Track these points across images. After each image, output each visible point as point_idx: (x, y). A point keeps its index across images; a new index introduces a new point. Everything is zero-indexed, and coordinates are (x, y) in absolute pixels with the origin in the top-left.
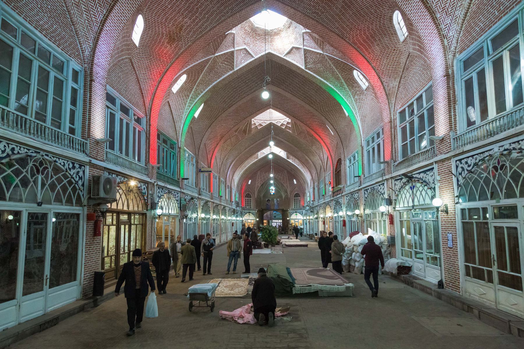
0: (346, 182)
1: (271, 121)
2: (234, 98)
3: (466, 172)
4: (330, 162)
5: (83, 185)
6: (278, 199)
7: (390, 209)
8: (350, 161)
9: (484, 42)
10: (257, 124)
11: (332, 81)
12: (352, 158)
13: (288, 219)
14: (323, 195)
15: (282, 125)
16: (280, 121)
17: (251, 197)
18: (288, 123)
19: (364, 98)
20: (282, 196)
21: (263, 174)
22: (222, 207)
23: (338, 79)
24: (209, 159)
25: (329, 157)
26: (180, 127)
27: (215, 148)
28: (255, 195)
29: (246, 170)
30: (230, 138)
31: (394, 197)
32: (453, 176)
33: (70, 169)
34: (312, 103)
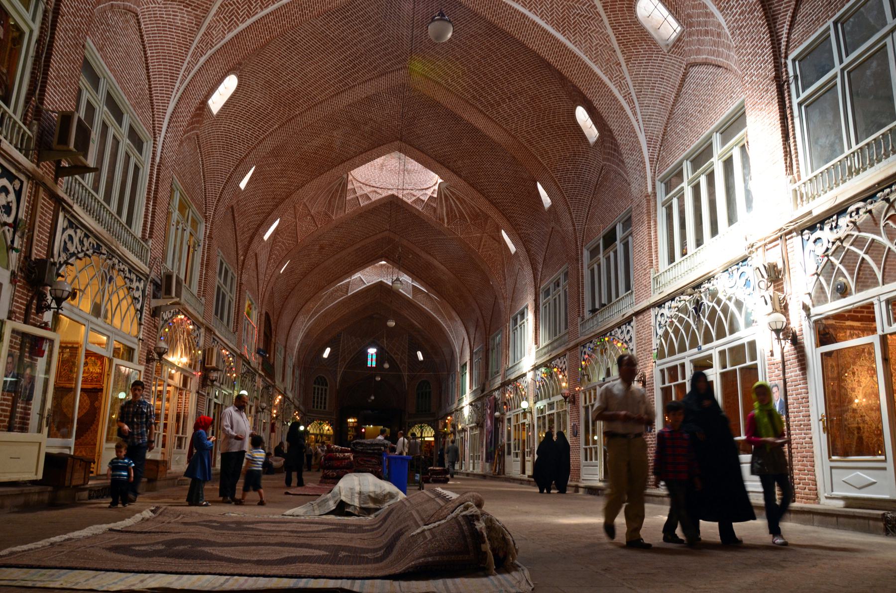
1: (395, 192)
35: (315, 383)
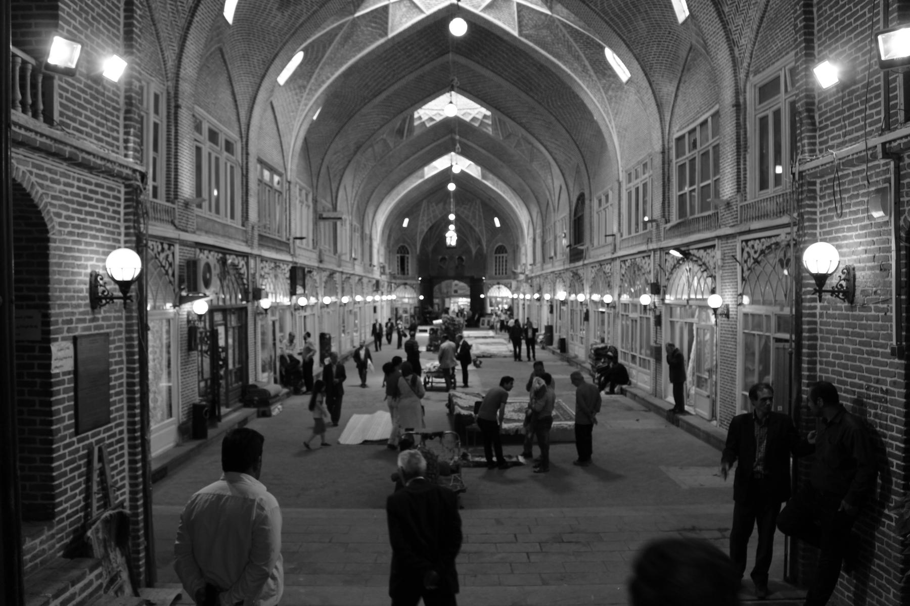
0: (591, 240)
2: (384, 78)
3: (752, 261)
4: (564, 196)
5: (173, 275)
6: (464, 258)
7: (656, 299)
8: (600, 201)
9: (781, 69)
10: (425, 118)
11: (567, 62)
12: (603, 198)
13: (482, 296)
14: (551, 258)
15: (474, 119)
16: (469, 111)
17: (408, 253)
18: (485, 117)
19: (624, 97)
20: (470, 252)
21: (433, 207)
22: (357, 278)
23: (578, 58)
24: (334, 190)
25: (564, 187)
26: (289, 144)
27: (345, 169)
28: (416, 249)
29: (401, 201)
31: (663, 282)
32: (738, 264)
33: (159, 253)
34: (531, 89)
35: (398, 253)
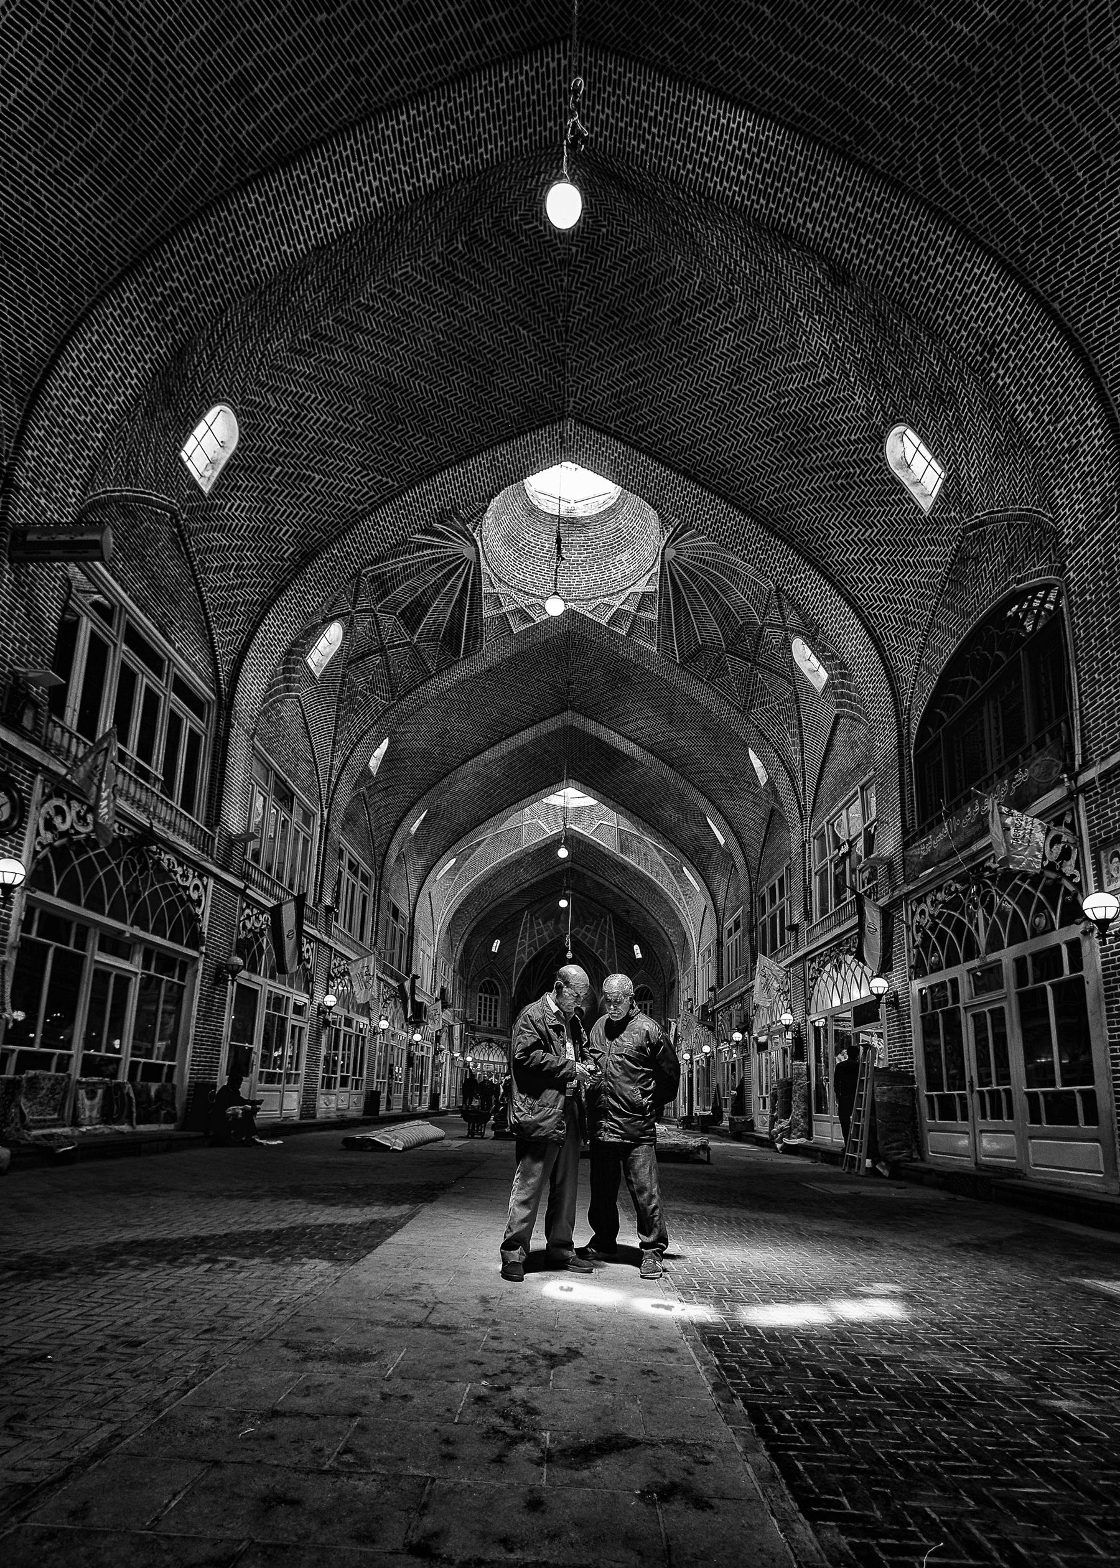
27: (266, 606)
30: (382, 650)
35: (481, 991)
